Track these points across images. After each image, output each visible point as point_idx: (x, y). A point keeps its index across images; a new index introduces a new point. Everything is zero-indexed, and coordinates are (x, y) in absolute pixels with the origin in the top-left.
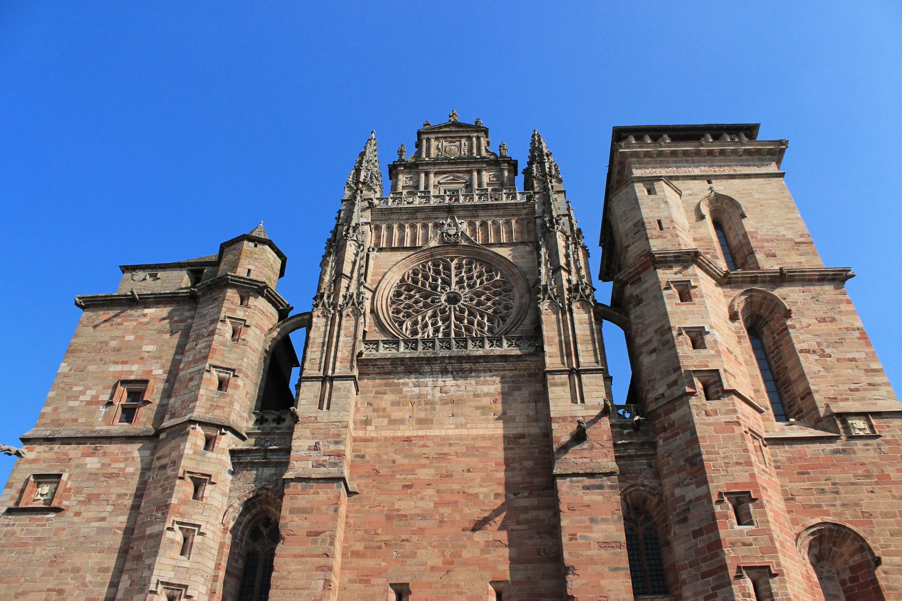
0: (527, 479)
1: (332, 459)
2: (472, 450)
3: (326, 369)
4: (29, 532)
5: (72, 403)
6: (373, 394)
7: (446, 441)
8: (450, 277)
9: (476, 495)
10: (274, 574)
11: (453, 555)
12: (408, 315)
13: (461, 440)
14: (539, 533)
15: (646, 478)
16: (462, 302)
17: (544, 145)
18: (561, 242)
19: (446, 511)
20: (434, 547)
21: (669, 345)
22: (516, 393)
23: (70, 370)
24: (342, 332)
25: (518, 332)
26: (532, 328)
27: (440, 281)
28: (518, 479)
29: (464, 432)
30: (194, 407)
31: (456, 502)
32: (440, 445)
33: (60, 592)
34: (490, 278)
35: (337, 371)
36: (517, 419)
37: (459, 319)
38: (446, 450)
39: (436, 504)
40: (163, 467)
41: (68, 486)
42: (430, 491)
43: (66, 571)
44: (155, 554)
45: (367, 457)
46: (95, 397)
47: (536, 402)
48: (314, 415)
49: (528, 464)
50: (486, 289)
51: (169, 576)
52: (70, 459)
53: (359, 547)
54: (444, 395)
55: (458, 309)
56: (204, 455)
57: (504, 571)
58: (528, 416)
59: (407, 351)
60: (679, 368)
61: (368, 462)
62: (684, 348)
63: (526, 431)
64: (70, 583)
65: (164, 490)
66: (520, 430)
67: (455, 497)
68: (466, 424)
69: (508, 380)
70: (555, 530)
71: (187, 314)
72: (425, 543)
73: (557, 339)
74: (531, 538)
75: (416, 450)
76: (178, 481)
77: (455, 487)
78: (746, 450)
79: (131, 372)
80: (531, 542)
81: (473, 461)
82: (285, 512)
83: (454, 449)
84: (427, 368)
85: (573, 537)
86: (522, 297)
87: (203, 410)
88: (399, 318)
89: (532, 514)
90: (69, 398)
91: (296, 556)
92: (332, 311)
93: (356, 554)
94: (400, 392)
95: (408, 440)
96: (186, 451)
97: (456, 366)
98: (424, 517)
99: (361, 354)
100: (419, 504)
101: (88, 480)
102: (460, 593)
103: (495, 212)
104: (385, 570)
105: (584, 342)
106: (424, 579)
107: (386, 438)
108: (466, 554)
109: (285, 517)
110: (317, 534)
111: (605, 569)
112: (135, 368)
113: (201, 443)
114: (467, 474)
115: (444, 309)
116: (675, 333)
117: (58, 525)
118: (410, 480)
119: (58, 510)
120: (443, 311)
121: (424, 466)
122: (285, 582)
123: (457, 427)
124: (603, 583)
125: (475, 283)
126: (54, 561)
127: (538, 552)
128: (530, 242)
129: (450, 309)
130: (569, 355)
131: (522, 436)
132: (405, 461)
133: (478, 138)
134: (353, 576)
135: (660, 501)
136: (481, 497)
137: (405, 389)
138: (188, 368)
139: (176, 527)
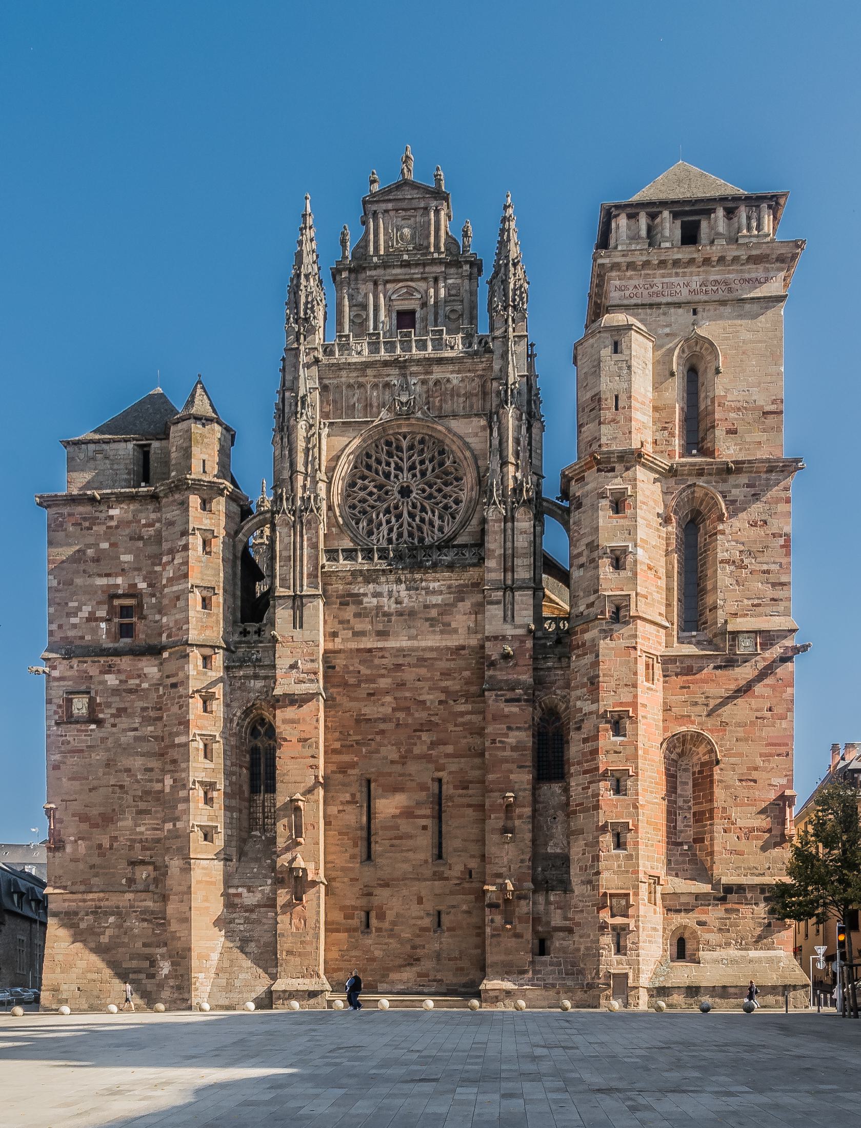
0: (465, 688)
2: (422, 661)
4: (81, 741)
5: (74, 620)
6: (337, 606)
8: (401, 459)
9: (424, 702)
10: (277, 772)
11: (406, 752)
12: (364, 512)
13: (413, 651)
14: (471, 734)
15: (558, 688)
16: (414, 495)
17: (514, 237)
19: (401, 715)
20: (393, 745)
22: (460, 604)
23: (59, 583)
25: (465, 534)
26: (479, 529)
27: (393, 465)
29: (415, 643)
30: (188, 629)
31: (409, 708)
32: (396, 656)
33: (122, 787)
34: (441, 464)
35: (305, 588)
36: (460, 631)
37: (412, 516)
38: (401, 661)
39: (394, 710)
40: (174, 686)
41: (98, 701)
42: (388, 699)
43: (120, 771)
45: (337, 668)
48: (290, 634)
49: (466, 674)
50: (438, 477)
51: (202, 776)
52: (91, 677)
54: (399, 606)
55: (410, 503)
56: (205, 674)
58: (469, 628)
59: (364, 562)
61: (339, 672)
64: (127, 780)
65: (181, 707)
66: (461, 642)
67: (408, 704)
68: (417, 636)
69: (453, 590)
71: (153, 516)
72: (386, 742)
74: (465, 737)
75: (377, 661)
76: (190, 700)
77: (408, 694)
81: (423, 671)
82: (278, 723)
83: (408, 660)
84: (383, 579)
86: (472, 489)
87: (196, 632)
88: (355, 515)
89: (468, 717)
90: (69, 615)
92: (293, 518)
93: (335, 751)
94: (361, 603)
95: (370, 651)
96: (191, 673)
97: (408, 576)
98: (384, 720)
99: (323, 567)
100: (381, 709)
101: (112, 695)
103: (451, 368)
104: (357, 763)
106: (386, 770)
107: (351, 649)
108: (417, 750)
109: (279, 727)
112: (119, 580)
113: (200, 662)
115: (397, 503)
117: (101, 735)
118: (373, 689)
120: (396, 507)
121: (383, 676)
122: (286, 778)
123: (410, 638)
125: (427, 469)
127: (470, 750)
128: (485, 415)
129: (403, 503)
131: (463, 648)
134: (334, 768)
135: (567, 708)
136: (428, 704)
137: (365, 600)
138: (172, 586)
139: (198, 738)
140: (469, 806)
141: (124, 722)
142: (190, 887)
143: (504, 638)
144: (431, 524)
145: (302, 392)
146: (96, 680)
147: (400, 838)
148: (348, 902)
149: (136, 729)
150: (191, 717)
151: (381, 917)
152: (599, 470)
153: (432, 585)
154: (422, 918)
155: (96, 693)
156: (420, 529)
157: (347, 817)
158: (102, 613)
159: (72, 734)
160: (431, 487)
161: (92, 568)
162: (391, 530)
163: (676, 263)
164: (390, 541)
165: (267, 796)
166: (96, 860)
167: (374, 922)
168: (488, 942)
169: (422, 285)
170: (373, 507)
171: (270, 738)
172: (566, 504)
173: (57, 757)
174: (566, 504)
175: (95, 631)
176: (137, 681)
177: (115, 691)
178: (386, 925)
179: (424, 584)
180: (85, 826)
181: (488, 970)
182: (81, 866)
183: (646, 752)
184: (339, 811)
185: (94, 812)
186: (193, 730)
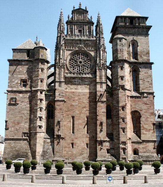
1: (62, 97)
2: (84, 95)
3: (60, 79)
7: (80, 93)
8: (80, 57)
9: (84, 102)
12: (72, 66)
18: (101, 52)
19: (80, 105)
21: (117, 79)
24: (62, 72)
28: (91, 100)
29: (82, 91)
31: (81, 103)
33: (22, 117)
37: (82, 67)
38: (80, 94)
39: (78, 104)
42: (77, 101)
44: (37, 112)
46: (18, 82)
47: (94, 86)
49: (93, 97)
53: (67, 110)
57: (88, 114)
60: (118, 84)
62: (120, 80)
63: (92, 91)
64: (23, 116)
65: (36, 102)
67: (81, 103)
70: (96, 109)
71: (31, 64)
73: (99, 75)
75: (75, 94)
77: (81, 101)
78: (126, 99)
79: (23, 77)
80: (92, 110)
81: (84, 96)
82: (56, 105)
84: (76, 79)
85: (99, 111)
86: (93, 63)
89: (93, 106)
91: (58, 112)
93: (66, 111)
95: (73, 92)
98: (76, 106)
102: (82, 118)
103: (89, 41)
105: (104, 76)
106: (77, 116)
107: (70, 92)
110: (61, 109)
111: (103, 116)
113: (40, 93)
114: (83, 99)
116: (119, 77)
119: (18, 104)
120: (79, 65)
121: (76, 97)
123: (82, 90)
124: (102, 118)
125: (85, 59)
126: (19, 112)
130: (101, 79)
131: (92, 92)
132: (73, 96)
133: (86, 14)
140: (93, 123)
141: (23, 104)
142: (36, 138)
143: (100, 91)
144: (86, 69)
145: (61, 44)
146: (18, 95)
147: (79, 129)
148: (68, 142)
149: (25, 105)
150: (38, 104)
151: (75, 144)
152: (118, 62)
153: (86, 80)
154: (84, 146)
155: (18, 98)
156: (83, 70)
157: (68, 125)
158: (19, 82)
159: (12, 107)
160: (85, 62)
161: (18, 74)
162: (78, 69)
163: (130, 27)
164: (77, 71)
165: (51, 120)
166: (16, 132)
167: (74, 146)
168: (98, 151)
169: (83, 26)
170: (74, 65)
171: (52, 108)
172: (110, 66)
173: (9, 110)
174: (110, 66)
175: (18, 85)
176: (26, 96)
177: (22, 98)
178: (76, 147)
179: (84, 80)
180: (13, 125)
181: (98, 156)
182: (12, 133)
183: (128, 114)
184: (67, 123)
185: (16, 122)
186: (38, 107)
